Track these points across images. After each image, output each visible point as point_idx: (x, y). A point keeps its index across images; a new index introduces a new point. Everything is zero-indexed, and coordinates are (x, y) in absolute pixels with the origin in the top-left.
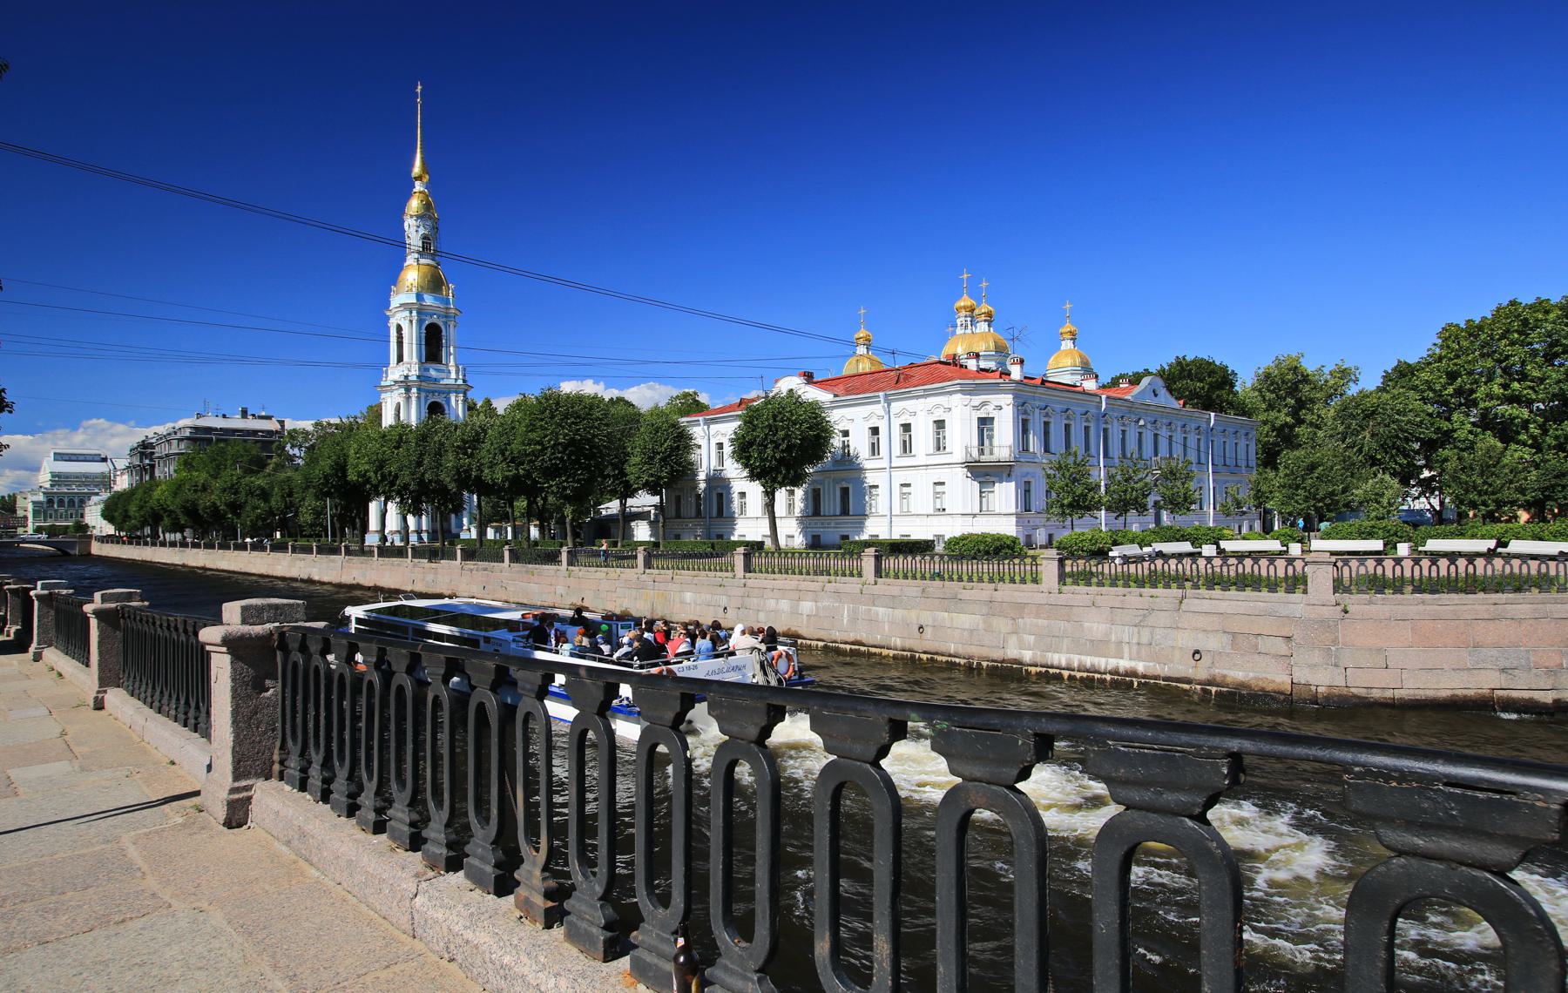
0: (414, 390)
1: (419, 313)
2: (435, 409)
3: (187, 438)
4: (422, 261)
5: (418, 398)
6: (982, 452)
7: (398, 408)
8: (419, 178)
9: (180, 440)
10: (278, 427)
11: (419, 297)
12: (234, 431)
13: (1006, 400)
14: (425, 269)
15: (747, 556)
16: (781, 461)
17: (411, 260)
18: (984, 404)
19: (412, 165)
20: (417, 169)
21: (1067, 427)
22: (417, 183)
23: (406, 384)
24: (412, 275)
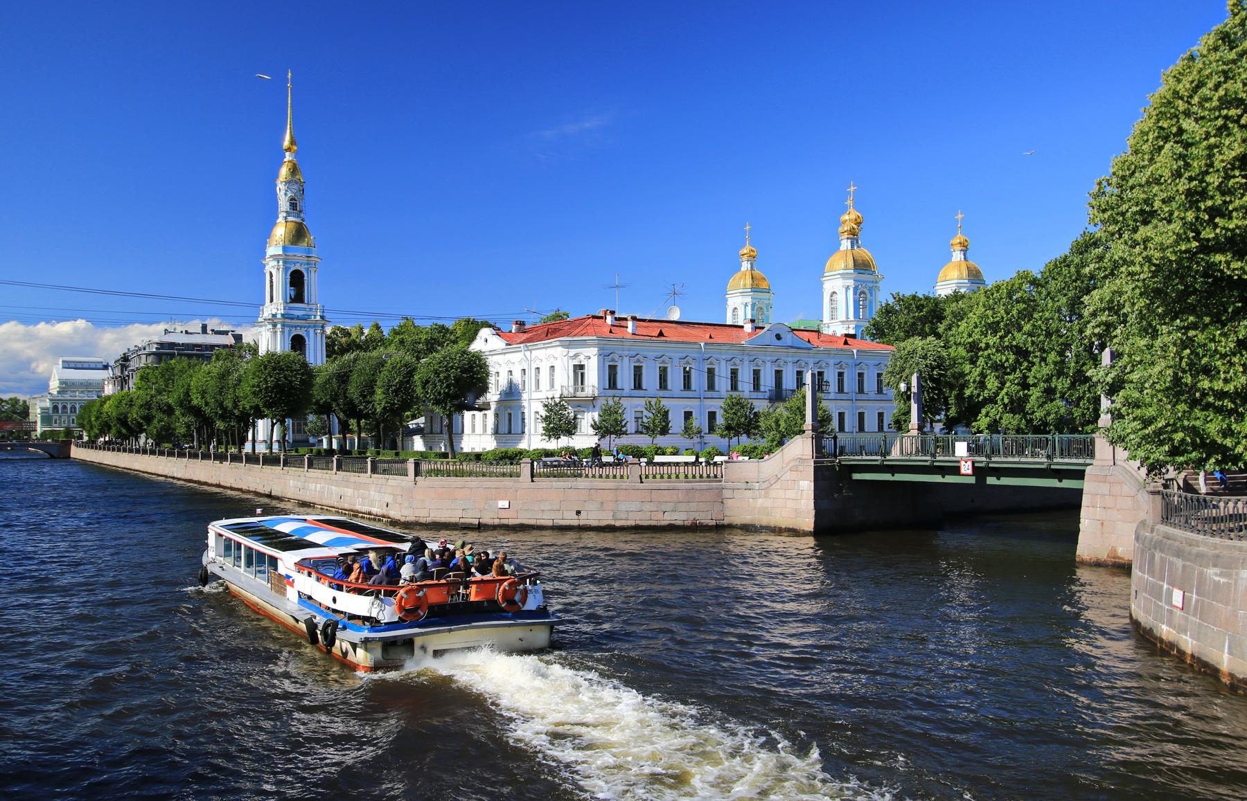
0: (279, 326)
1: (285, 262)
2: (298, 343)
3: (153, 353)
4: (290, 219)
5: (283, 332)
6: (576, 390)
7: (267, 340)
8: (289, 149)
11: (285, 248)
13: (593, 351)
14: (291, 225)
15: (417, 465)
16: (447, 395)
17: (281, 219)
18: (576, 355)
20: (286, 143)
22: (287, 154)
23: (273, 321)
24: (280, 231)
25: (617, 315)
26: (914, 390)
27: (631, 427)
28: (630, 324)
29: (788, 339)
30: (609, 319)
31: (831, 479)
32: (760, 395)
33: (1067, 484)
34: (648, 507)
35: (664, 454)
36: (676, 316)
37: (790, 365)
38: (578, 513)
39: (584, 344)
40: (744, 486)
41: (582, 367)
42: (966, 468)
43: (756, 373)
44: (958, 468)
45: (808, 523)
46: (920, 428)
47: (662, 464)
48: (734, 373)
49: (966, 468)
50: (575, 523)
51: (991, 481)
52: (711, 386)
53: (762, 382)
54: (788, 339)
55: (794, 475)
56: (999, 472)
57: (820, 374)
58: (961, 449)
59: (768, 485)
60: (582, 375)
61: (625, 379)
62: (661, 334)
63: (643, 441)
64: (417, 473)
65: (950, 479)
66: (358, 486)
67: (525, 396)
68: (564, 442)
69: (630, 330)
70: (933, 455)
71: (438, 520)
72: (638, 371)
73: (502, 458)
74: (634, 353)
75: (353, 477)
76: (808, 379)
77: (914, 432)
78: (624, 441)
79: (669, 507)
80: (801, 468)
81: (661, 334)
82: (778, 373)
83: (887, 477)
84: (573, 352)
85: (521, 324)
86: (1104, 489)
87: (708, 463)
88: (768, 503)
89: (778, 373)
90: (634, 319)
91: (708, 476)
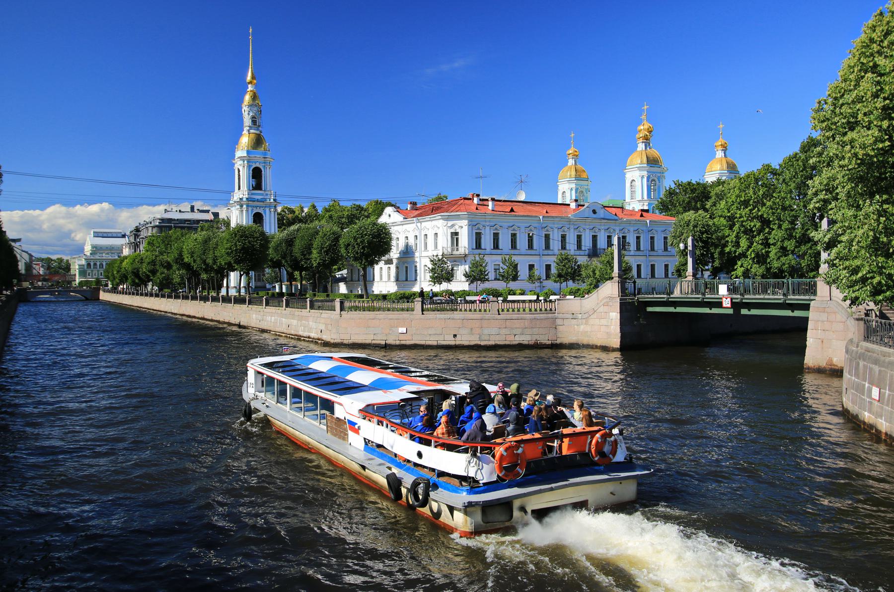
1: (248, 162)
2: (258, 218)
4: (252, 131)
5: (247, 211)
7: (237, 217)
8: (251, 83)
9: (153, 227)
10: (212, 217)
11: (248, 152)
12: (186, 221)
13: (464, 223)
14: (252, 136)
15: (342, 303)
17: (245, 132)
18: (453, 226)
19: (246, 75)
20: (249, 78)
21: (514, 236)
22: (250, 86)
23: (240, 203)
24: (245, 140)
25: (481, 197)
26: (690, 248)
27: (491, 276)
28: (490, 203)
29: (601, 213)
30: (476, 200)
31: (632, 311)
32: (581, 252)
33: (798, 313)
34: (504, 331)
35: (514, 294)
36: (522, 197)
37: (603, 231)
38: (455, 336)
39: (458, 218)
40: (571, 316)
41: (457, 234)
42: (727, 303)
43: (579, 237)
44: (721, 303)
45: (616, 342)
46: (694, 275)
47: (514, 301)
48: (563, 237)
49: (727, 303)
50: (453, 343)
51: (744, 312)
52: (547, 247)
53: (583, 244)
54: (601, 213)
55: (606, 309)
56: (749, 306)
57: (624, 237)
58: (723, 289)
59: (587, 316)
60: (457, 239)
61: (487, 242)
62: (512, 210)
63: (500, 285)
64: (342, 309)
65: (715, 311)
66: (300, 318)
67: (417, 254)
68: (444, 286)
69: (490, 207)
70: (704, 294)
71: (357, 341)
72: (496, 236)
73: (401, 298)
74: (493, 224)
75: (297, 312)
76: (615, 241)
77: (690, 278)
78: (487, 285)
79: (518, 331)
80: (611, 304)
81: (512, 210)
82: (595, 238)
83: (671, 309)
84: (450, 223)
85: (414, 204)
86: (824, 317)
87: (545, 301)
88: (588, 328)
89: (595, 238)
90: (493, 200)
91: (546, 310)
